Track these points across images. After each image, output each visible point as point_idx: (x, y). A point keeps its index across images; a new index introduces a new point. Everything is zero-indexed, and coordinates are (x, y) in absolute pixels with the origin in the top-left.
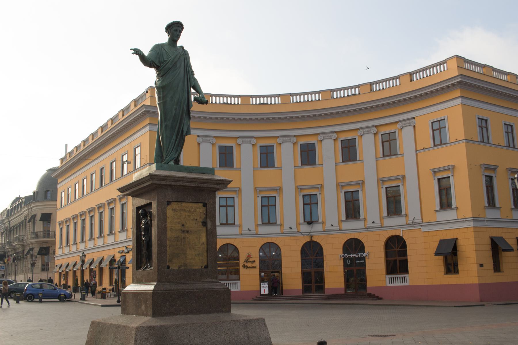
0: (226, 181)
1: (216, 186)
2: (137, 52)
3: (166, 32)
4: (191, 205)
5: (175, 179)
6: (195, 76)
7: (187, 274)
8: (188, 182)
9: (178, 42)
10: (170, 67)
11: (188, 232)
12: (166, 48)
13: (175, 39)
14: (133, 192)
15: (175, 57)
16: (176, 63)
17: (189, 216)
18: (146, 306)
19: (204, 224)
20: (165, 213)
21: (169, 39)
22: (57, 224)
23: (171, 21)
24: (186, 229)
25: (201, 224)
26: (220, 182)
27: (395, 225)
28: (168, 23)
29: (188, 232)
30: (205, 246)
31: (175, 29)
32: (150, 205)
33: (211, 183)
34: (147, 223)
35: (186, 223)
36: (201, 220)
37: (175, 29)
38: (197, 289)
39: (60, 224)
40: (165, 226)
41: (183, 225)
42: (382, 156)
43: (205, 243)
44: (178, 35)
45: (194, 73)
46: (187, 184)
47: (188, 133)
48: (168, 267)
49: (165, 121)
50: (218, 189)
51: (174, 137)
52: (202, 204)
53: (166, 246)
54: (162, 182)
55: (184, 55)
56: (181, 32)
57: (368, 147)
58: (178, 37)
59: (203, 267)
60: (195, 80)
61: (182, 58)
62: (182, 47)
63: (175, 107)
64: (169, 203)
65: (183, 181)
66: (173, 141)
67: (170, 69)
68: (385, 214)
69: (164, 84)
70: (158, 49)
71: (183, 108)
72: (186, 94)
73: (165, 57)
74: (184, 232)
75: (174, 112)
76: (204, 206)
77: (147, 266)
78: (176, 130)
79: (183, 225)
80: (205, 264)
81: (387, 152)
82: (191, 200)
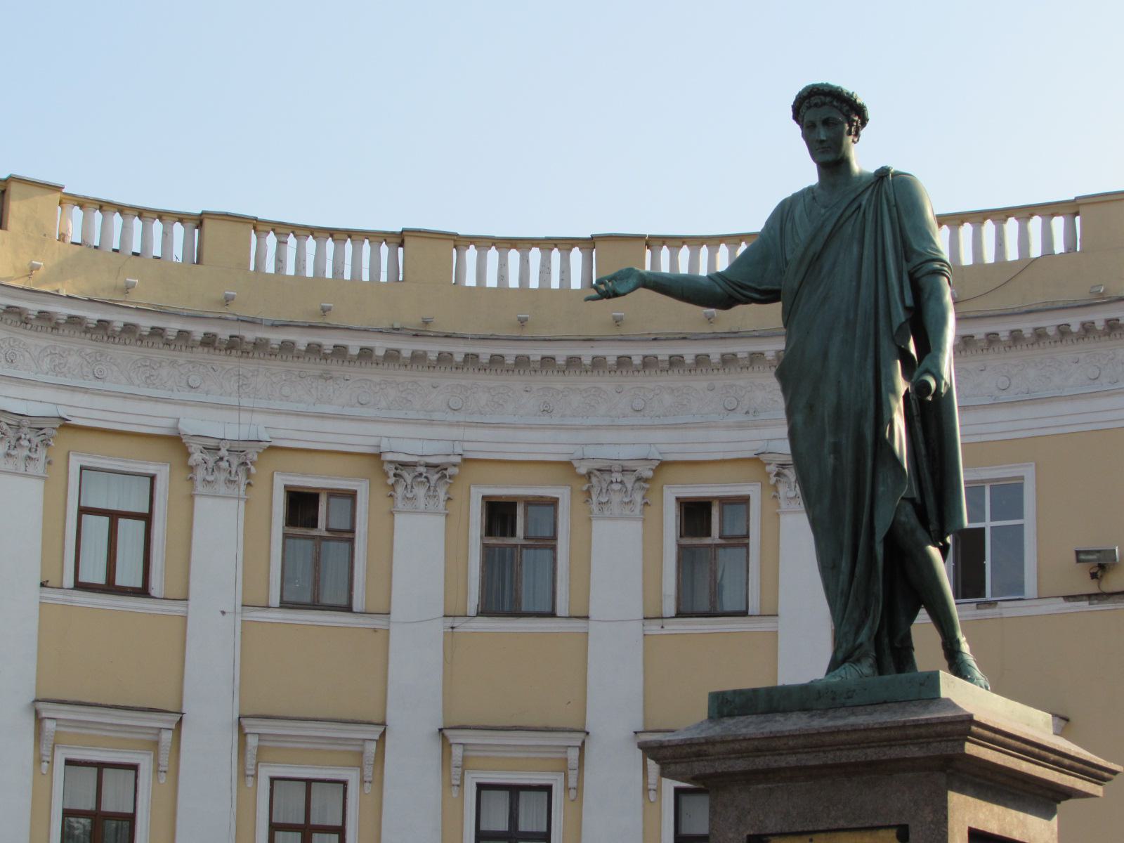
8: (793, 751)
10: (796, 285)
16: (818, 257)
26: (923, 731)
31: (827, 115)
33: (891, 742)
37: (827, 115)
46: (792, 760)
51: (845, 565)
52: (893, 833)
62: (883, 174)
63: (829, 439)
66: (844, 578)
67: (797, 294)
71: (860, 438)
72: (870, 374)
75: (830, 460)
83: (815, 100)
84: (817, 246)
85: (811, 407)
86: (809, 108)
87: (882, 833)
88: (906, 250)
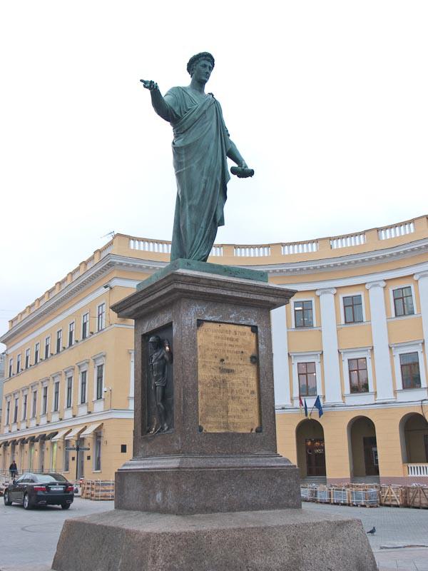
0: (288, 291)
1: (272, 299)
2: (152, 87)
3: (189, 70)
4: (233, 328)
5: (210, 283)
6: (231, 138)
7: (230, 441)
8: (231, 289)
9: (206, 84)
10: (197, 117)
11: (229, 371)
12: (190, 92)
13: (204, 78)
14: (138, 310)
15: (203, 105)
17: (230, 345)
18: (164, 495)
19: (255, 360)
20: (195, 342)
21: (193, 82)
22: (4, 398)
23: (196, 53)
24: (227, 367)
25: (249, 359)
26: (279, 292)
27: (412, 400)
28: (192, 56)
29: (229, 371)
30: (256, 396)
31: (201, 66)
32: (169, 326)
34: (163, 357)
35: (227, 358)
36: (250, 354)
37: (201, 66)
38: (247, 467)
39: (6, 398)
40: (195, 359)
41: (222, 360)
42: (393, 315)
43: (256, 391)
44: (207, 73)
45: (229, 132)
47: (222, 223)
48: (201, 429)
49: (189, 199)
50: (275, 306)
51: (203, 225)
53: (197, 393)
54: (192, 288)
55: (214, 107)
56: (211, 69)
57: (377, 304)
58: (208, 75)
59: (254, 431)
60: (231, 142)
61: (214, 107)
63: (204, 177)
64: (200, 323)
65: (224, 288)
66: (201, 230)
68: (399, 386)
69: (188, 142)
70: (178, 92)
71: (216, 181)
73: (188, 105)
74: (223, 371)
75: (203, 185)
76: (252, 331)
77: (162, 428)
78: (206, 214)
79: (222, 360)
80: (257, 425)
81: (400, 311)
82: (233, 322)
83: (208, 58)
84: (205, 108)
85: (200, 163)
86: (204, 59)
87: (246, 327)
88: (223, 127)
